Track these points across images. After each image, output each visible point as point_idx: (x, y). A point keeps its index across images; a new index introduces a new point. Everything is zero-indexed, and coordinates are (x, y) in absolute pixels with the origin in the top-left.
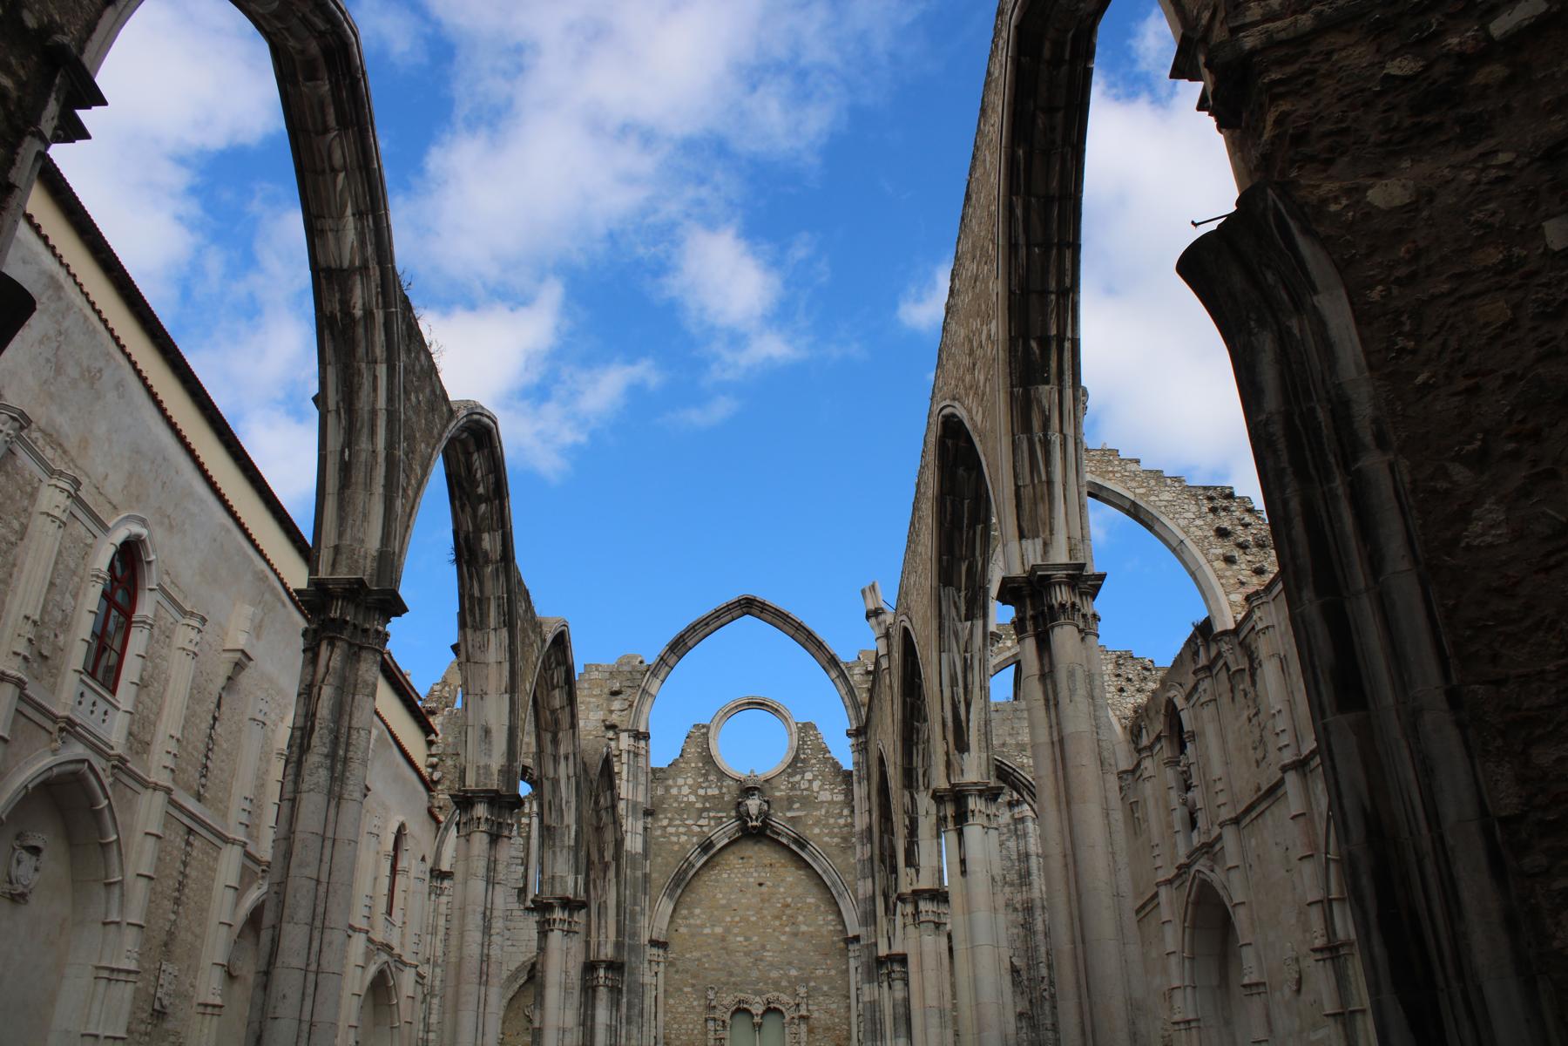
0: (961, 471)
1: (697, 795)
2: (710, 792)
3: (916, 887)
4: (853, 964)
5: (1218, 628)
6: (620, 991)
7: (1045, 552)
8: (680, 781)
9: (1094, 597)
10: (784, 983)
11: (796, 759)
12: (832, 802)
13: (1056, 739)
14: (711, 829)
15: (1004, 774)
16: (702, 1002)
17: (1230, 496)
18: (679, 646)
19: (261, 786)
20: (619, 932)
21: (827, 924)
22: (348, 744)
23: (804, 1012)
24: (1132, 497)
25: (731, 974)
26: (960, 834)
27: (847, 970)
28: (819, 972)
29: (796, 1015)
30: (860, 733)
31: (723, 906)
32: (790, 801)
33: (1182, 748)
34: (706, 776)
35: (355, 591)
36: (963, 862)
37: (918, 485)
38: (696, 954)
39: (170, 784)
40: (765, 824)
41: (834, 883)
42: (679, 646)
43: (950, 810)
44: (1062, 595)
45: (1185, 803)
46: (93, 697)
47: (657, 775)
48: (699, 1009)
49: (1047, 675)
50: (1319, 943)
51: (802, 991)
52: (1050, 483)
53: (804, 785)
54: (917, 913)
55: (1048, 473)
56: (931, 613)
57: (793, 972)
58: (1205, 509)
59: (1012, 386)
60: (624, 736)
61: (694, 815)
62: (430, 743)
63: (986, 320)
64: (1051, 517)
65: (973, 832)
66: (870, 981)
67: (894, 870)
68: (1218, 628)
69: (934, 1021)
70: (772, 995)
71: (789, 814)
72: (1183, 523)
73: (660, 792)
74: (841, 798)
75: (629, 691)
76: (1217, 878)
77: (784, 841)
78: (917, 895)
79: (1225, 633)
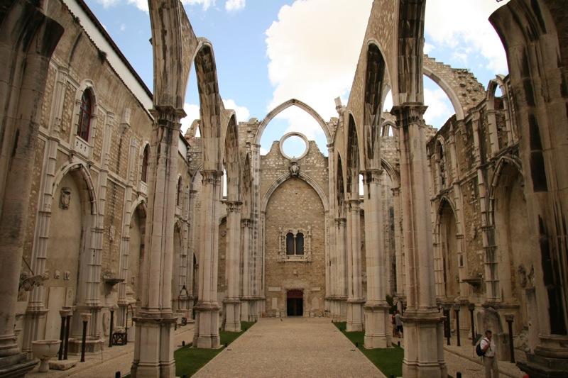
0: (375, 63)
3: (350, 199)
4: (326, 219)
5: (458, 119)
6: (252, 228)
7: (408, 98)
8: (270, 160)
9: (423, 113)
11: (308, 153)
13: (409, 162)
15: (383, 164)
17: (466, 73)
18: (270, 116)
19: (136, 167)
20: (252, 210)
22: (170, 163)
23: (310, 234)
24: (432, 72)
26: (369, 186)
30: (331, 146)
33: (442, 157)
35: (168, 110)
36: (369, 195)
37: (358, 65)
38: (276, 216)
39: (107, 169)
40: (298, 174)
42: (270, 116)
43: (365, 178)
44: (413, 114)
45: (441, 175)
46: (82, 143)
47: (262, 158)
49: (406, 140)
50: (484, 225)
51: (309, 227)
52: (411, 73)
53: (311, 161)
54: (350, 207)
55: (411, 70)
56: (362, 111)
58: (457, 77)
59: (399, 38)
62: (188, 149)
63: (390, 11)
64: (411, 86)
65: (372, 185)
67: (343, 191)
68: (458, 119)
69: (354, 242)
72: (449, 81)
73: (264, 163)
74: (322, 166)
76: (451, 200)
78: (350, 202)
79: (460, 121)
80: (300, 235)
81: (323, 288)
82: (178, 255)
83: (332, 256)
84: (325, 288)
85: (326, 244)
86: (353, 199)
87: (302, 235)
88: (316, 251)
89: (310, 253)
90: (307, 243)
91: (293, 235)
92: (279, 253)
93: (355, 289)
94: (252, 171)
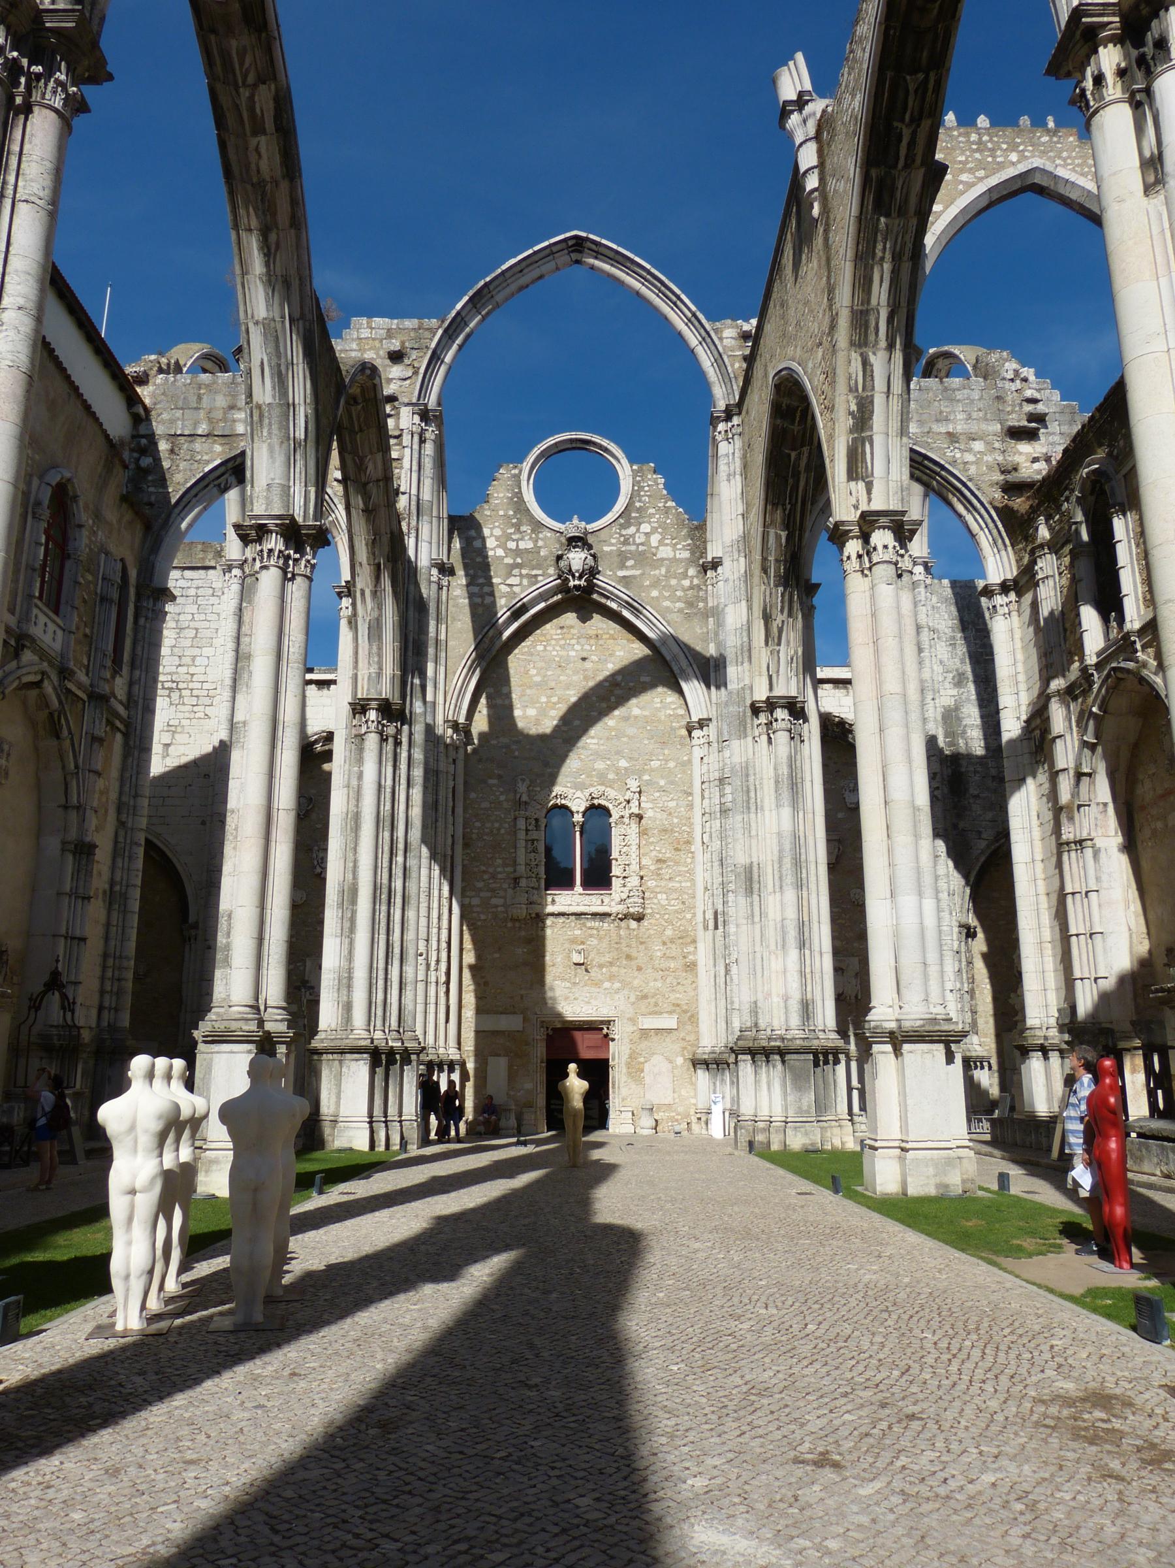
1: (505, 549)
2: (522, 545)
3: (864, 507)
4: (697, 753)
6: (398, 743)
10: (611, 776)
12: (674, 560)
14: (524, 589)
16: (511, 796)
21: (665, 706)
23: (636, 811)
25: (546, 764)
27: (690, 761)
28: (655, 764)
29: (627, 813)
31: (538, 685)
32: (622, 558)
34: (517, 526)
41: (675, 657)
48: (505, 805)
51: (633, 784)
57: (623, 763)
60: (405, 412)
61: (503, 572)
66: (743, 734)
70: (596, 790)
71: (621, 573)
74: (686, 554)
75: (414, 355)
77: (614, 606)
78: (868, 522)
80: (597, 811)
81: (690, 1017)
82: (53, 844)
83: (741, 859)
84: (693, 1019)
85: (697, 847)
86: (877, 505)
87: (606, 812)
88: (658, 874)
89: (634, 881)
90: (624, 844)
91: (572, 813)
92: (516, 880)
93: (910, 960)
94: (402, 503)
